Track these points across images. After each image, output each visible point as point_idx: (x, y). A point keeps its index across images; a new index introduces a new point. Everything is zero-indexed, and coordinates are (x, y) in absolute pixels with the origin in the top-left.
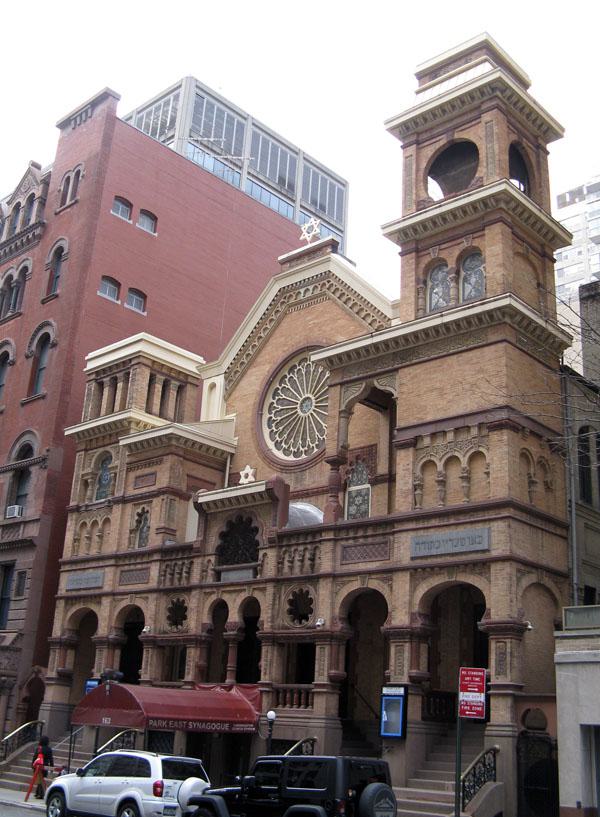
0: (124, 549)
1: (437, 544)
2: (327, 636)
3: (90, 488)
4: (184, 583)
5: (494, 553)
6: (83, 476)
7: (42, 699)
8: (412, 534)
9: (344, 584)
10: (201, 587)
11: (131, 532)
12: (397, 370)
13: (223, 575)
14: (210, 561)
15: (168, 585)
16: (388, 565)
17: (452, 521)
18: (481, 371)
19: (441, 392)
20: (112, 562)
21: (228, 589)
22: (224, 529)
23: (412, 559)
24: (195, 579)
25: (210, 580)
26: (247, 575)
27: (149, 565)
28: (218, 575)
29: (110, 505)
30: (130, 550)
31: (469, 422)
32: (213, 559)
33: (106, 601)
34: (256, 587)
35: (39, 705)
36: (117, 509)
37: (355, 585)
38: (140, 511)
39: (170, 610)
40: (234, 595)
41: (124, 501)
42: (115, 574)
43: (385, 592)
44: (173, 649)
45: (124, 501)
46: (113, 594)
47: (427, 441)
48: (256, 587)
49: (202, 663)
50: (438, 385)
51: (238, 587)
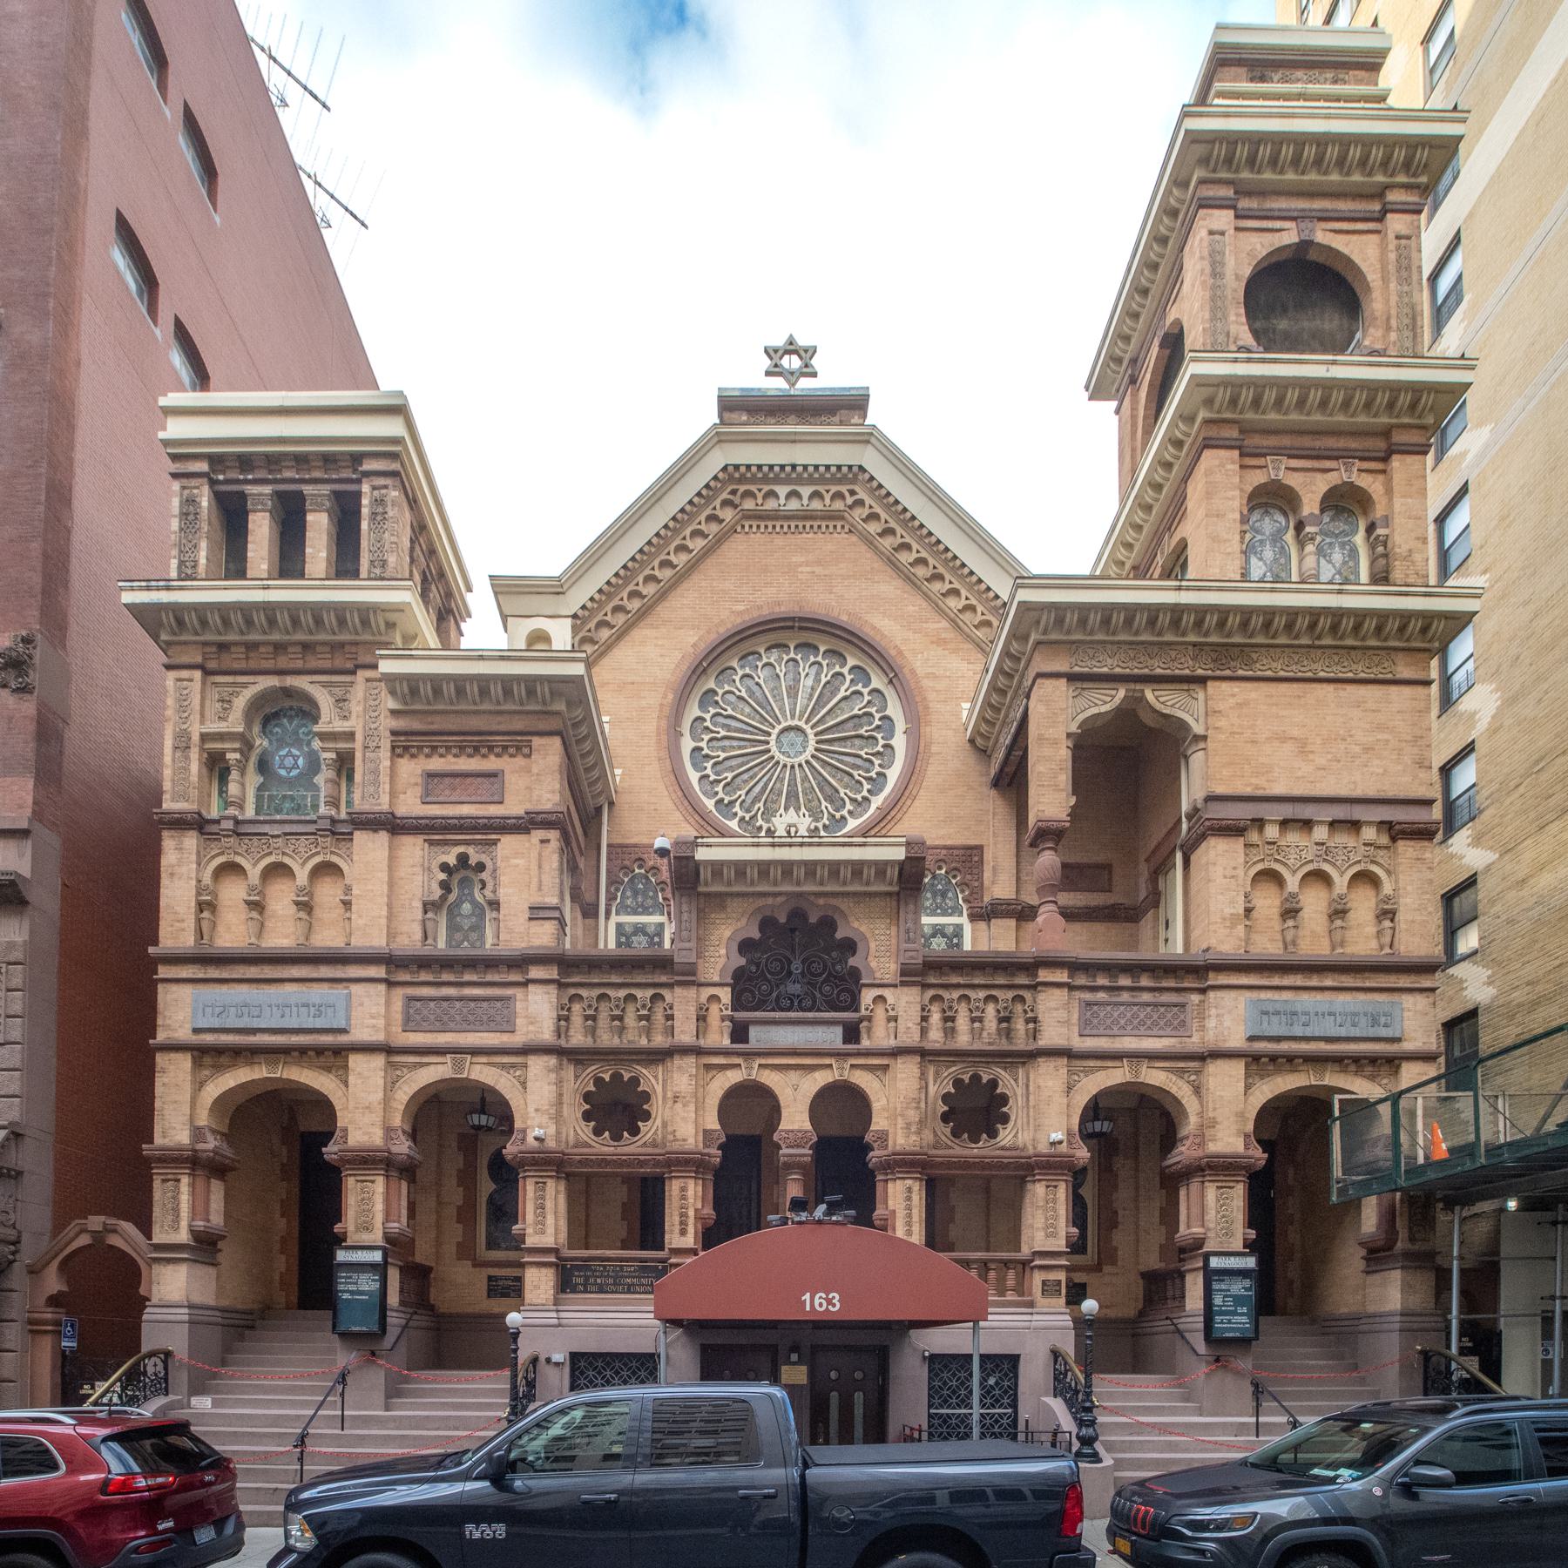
0: (410, 939)
1: (1303, 1019)
2: (1049, 1165)
3: (234, 775)
4: (659, 1041)
5: (1408, 1046)
6: (205, 737)
7: (142, 1302)
8: (1248, 994)
9: (1088, 1071)
10: (698, 1051)
11: (428, 906)
12: (1202, 681)
13: (754, 1032)
15: (578, 1038)
16: (1194, 1043)
17: (1328, 983)
18: (1380, 728)
19: (1303, 748)
20: (378, 971)
21: (770, 1061)
22: (755, 934)
23: (1251, 1039)
24: (685, 1034)
25: (719, 1036)
26: (832, 1037)
27: (509, 992)
28: (739, 1033)
29: (342, 830)
30: (427, 951)
31: (1358, 813)
32: (725, 995)
33: (367, 1073)
35: (141, 1313)
36: (370, 848)
37: (1116, 1076)
38: (451, 860)
39: (587, 1097)
40: (793, 1076)
41: (394, 826)
42: (388, 1003)
43: (1180, 1089)
44: (644, 1180)
45: (394, 826)
46: (388, 1050)
47: (1272, 832)
49: (709, 1211)
50: (1296, 732)
51: (800, 1059)
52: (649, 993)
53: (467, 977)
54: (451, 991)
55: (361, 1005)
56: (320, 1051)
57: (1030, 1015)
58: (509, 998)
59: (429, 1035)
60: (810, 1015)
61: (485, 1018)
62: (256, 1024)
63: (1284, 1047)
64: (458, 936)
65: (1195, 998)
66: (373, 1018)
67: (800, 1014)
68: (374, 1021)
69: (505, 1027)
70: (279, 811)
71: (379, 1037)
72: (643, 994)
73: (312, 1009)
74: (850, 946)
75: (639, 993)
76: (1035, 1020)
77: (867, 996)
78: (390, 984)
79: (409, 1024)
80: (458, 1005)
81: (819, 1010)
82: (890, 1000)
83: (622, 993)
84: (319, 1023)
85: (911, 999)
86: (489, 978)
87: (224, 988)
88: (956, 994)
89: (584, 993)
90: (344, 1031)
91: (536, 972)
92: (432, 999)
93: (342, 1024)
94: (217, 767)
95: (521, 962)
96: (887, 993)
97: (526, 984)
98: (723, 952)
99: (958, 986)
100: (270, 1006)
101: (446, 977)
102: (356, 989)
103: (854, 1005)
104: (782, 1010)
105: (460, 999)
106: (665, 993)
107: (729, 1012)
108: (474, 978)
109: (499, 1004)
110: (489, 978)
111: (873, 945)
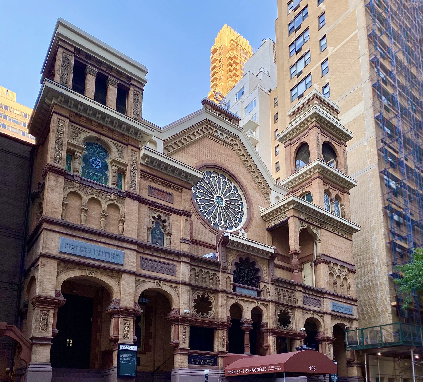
14: (229, 277)
15: (193, 283)
27: (175, 263)
34: (262, 302)
48: (262, 302)
52: (213, 272)
53: (162, 255)
54: (157, 259)
55: (128, 257)
56: (112, 270)
57: (294, 297)
58: (174, 265)
59: (149, 272)
60: (244, 286)
61: (167, 270)
62: (88, 255)
63: (337, 314)
64: (155, 240)
65: (322, 299)
66: (132, 262)
67: (247, 286)
68: (132, 264)
69: (173, 274)
70: (91, 178)
71: (134, 270)
72: (212, 272)
73: (111, 255)
74: (258, 270)
75: (210, 272)
76: (296, 298)
77: (262, 285)
78: (138, 252)
79: (142, 267)
80: (159, 264)
81: (251, 286)
82: (268, 287)
83: (206, 271)
84: (113, 261)
85: (273, 288)
86: (169, 257)
87: (74, 239)
88: (281, 289)
89: (196, 268)
90: (122, 265)
91: (183, 259)
92: (150, 260)
93: (122, 263)
94: (71, 155)
95: (179, 255)
96: (267, 285)
97: (180, 262)
98: (231, 265)
99: (281, 287)
100: (94, 250)
101: (155, 254)
102: (126, 251)
103: (258, 286)
104: (248, 285)
105: (159, 262)
106: (217, 273)
107: (233, 282)
108: (164, 256)
109: (171, 266)
110: (169, 257)
111: (264, 271)
